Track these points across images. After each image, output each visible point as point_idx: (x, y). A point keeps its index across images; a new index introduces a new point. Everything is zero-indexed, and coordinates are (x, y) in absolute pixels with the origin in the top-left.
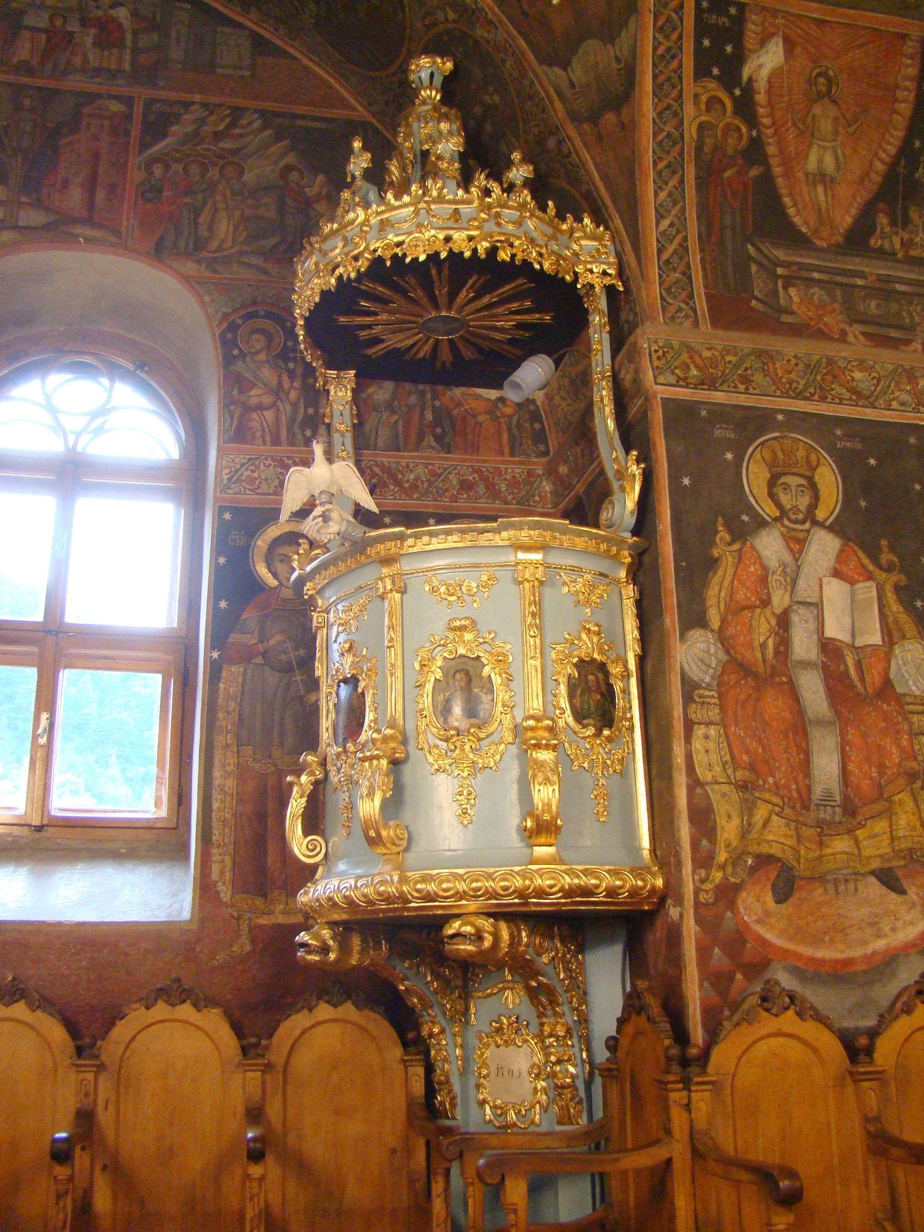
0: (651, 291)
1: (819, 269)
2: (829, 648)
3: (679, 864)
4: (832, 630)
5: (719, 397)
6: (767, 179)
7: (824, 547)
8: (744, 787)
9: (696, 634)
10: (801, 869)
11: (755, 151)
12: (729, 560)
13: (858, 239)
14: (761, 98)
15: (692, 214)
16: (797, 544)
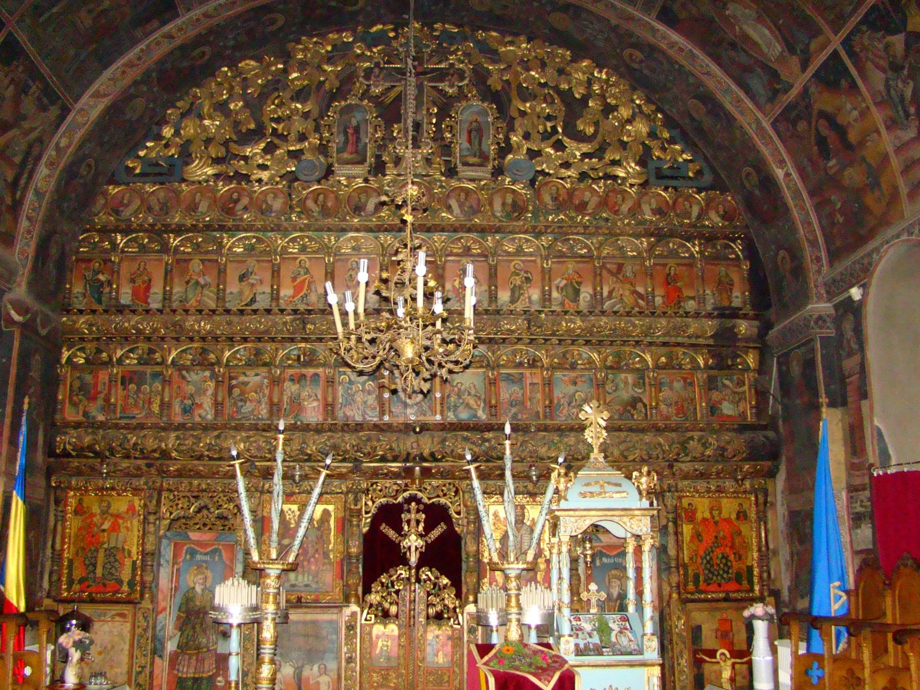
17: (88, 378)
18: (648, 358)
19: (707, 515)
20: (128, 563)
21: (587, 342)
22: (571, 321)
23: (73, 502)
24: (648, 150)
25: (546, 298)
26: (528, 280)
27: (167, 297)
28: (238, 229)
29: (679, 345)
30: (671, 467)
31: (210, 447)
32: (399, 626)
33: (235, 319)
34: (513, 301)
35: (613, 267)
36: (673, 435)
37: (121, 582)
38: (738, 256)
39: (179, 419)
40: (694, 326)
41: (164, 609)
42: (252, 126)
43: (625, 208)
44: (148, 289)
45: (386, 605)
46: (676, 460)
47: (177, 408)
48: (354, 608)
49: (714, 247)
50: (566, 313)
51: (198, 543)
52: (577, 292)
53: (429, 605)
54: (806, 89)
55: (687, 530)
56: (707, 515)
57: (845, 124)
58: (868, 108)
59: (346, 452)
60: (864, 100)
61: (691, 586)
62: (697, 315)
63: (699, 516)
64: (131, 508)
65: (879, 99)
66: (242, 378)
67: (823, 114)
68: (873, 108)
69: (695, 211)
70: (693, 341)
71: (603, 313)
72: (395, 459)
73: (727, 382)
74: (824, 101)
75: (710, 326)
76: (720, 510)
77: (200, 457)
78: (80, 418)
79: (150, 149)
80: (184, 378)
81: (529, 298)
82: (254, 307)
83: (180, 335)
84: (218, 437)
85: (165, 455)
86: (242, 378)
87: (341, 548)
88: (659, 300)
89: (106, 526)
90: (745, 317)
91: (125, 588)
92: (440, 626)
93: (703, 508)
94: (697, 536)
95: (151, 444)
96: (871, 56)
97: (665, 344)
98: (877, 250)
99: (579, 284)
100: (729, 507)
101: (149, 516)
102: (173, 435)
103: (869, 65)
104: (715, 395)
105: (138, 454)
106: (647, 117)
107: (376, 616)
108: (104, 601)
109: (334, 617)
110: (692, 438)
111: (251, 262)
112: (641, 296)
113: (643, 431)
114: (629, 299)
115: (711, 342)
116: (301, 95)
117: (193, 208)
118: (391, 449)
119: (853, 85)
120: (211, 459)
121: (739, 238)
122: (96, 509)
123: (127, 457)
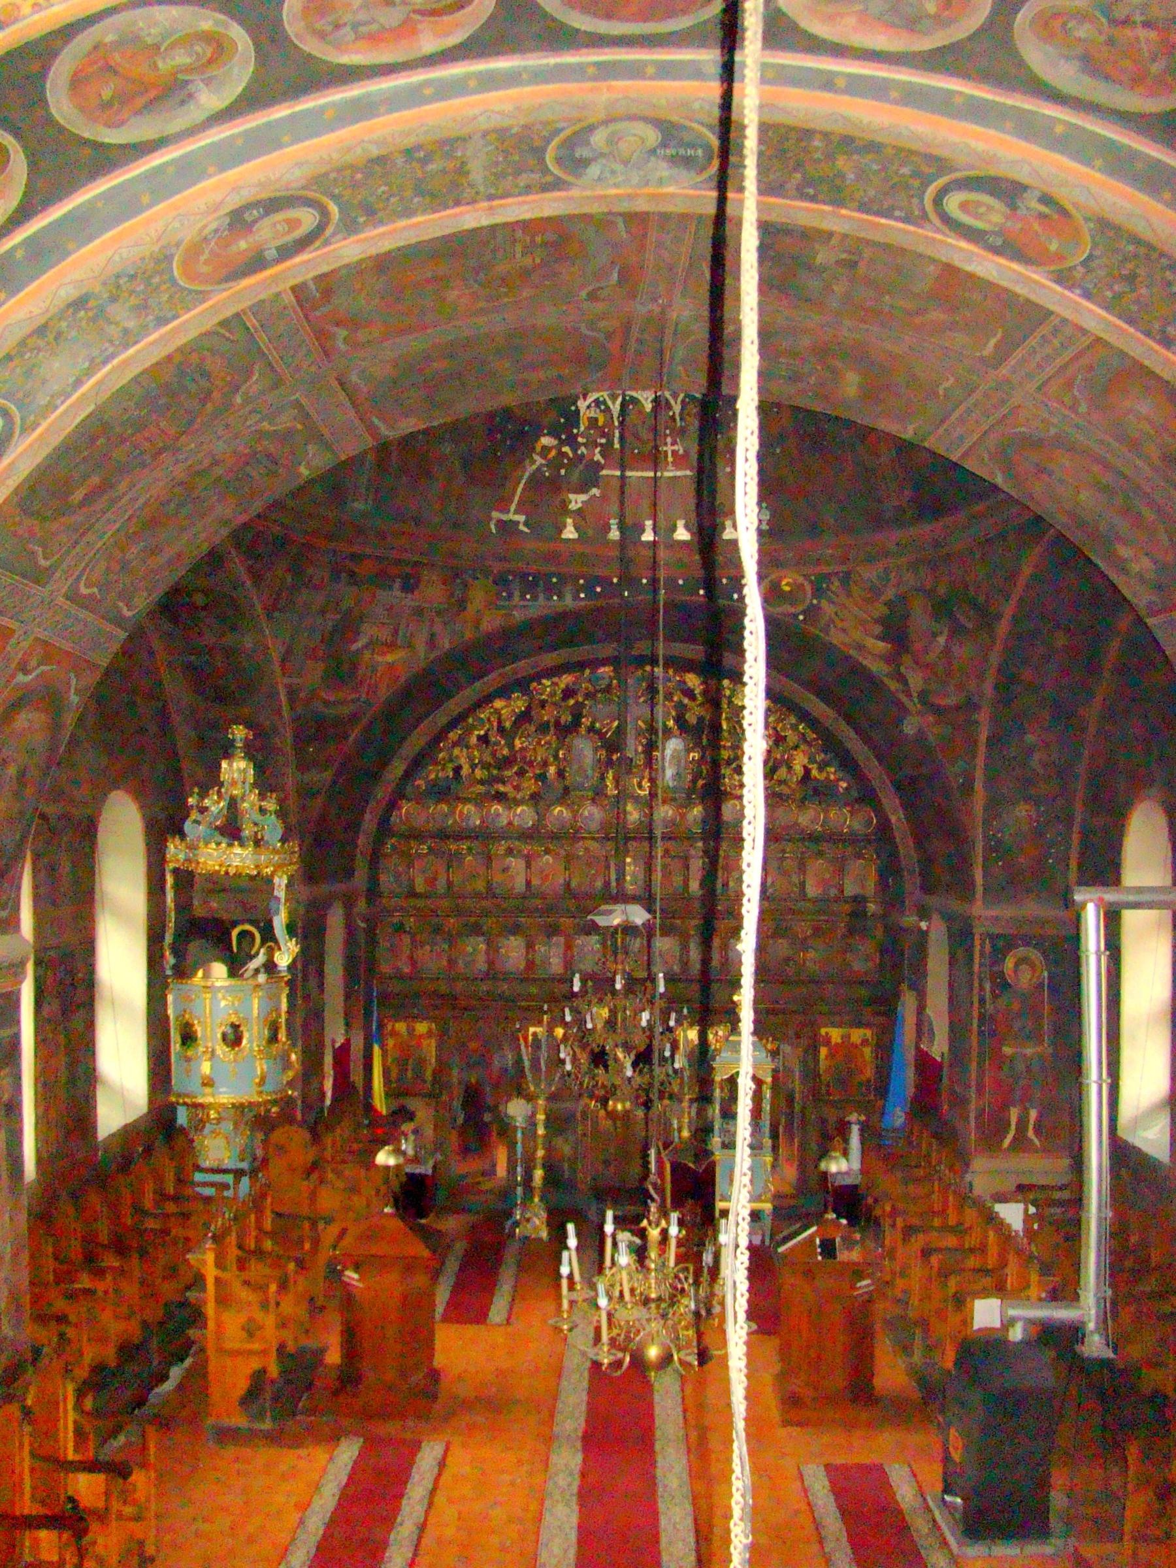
23: (389, 1027)
24: (807, 771)
27: (450, 884)
42: (506, 752)
44: (435, 879)
47: (461, 963)
48: (587, 1100)
55: (824, 1051)
63: (833, 1041)
64: (430, 1031)
76: (849, 1036)
79: (432, 773)
93: (836, 1034)
94: (831, 1055)
101: (442, 1035)
106: (809, 744)
116: (543, 728)
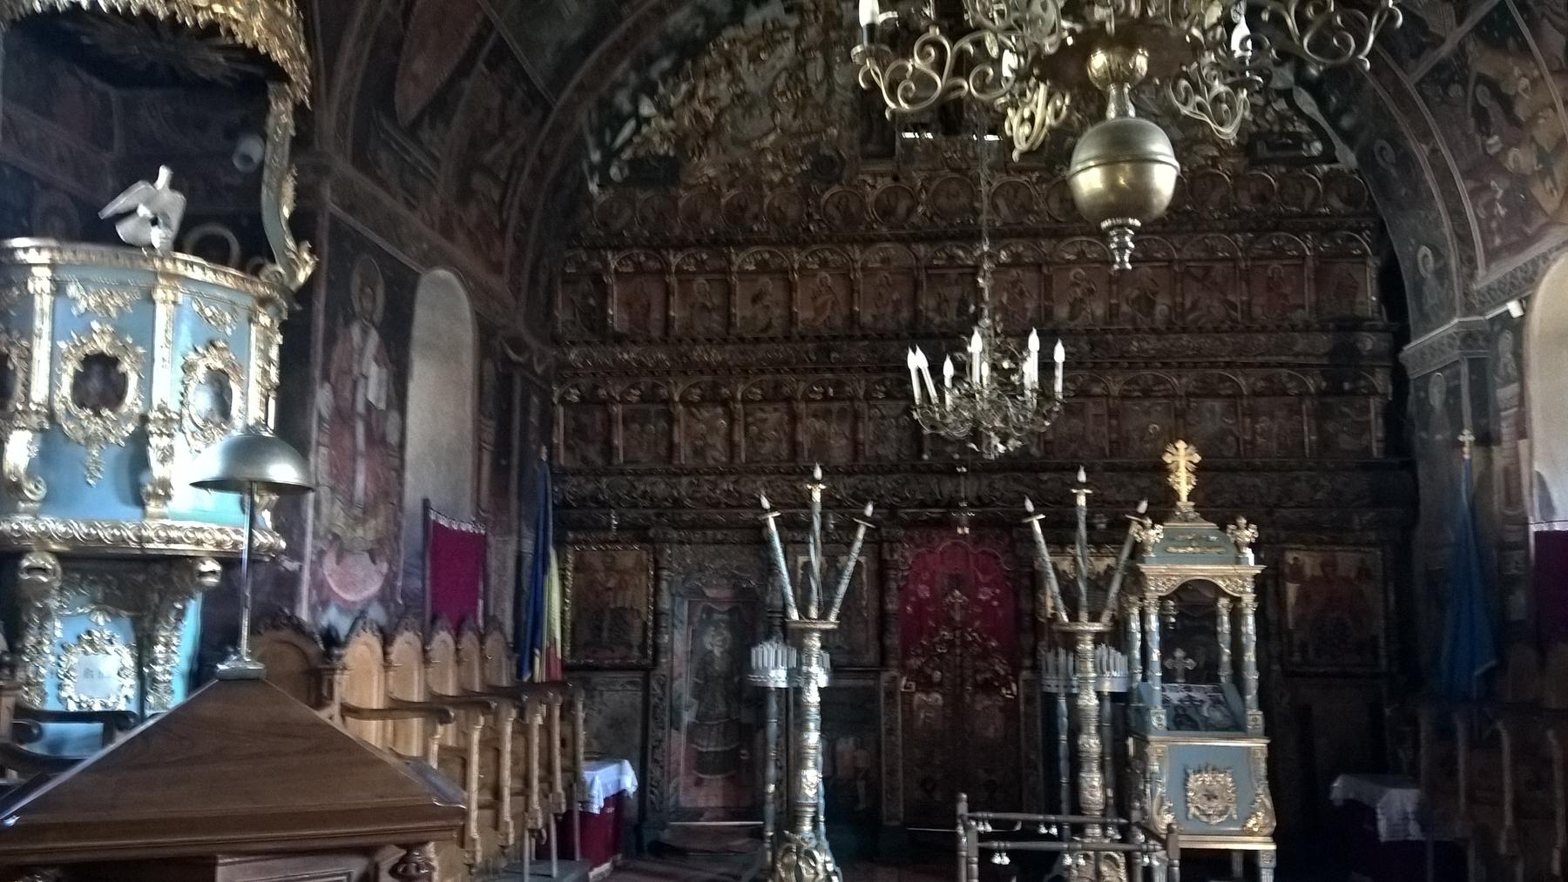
0: (328, 122)
1: (397, 143)
2: (368, 405)
3: (303, 534)
4: (371, 398)
5: (351, 220)
6: (395, 67)
7: (374, 338)
8: (333, 489)
9: (327, 386)
10: (346, 546)
11: (398, 46)
12: (341, 337)
13: (413, 129)
14: (415, 10)
15: (360, 75)
16: (365, 332)
17: (585, 419)
18: (1242, 381)
19: (1318, 572)
20: (637, 623)
21: (1165, 365)
22: (1144, 339)
25: (1113, 312)
26: (1091, 291)
28: (749, 243)
29: (1281, 365)
30: (1269, 514)
31: (728, 493)
32: (943, 695)
33: (749, 347)
34: (1072, 317)
35: (1199, 273)
36: (1275, 475)
37: (630, 646)
38: (1365, 251)
39: (691, 463)
40: (1301, 343)
41: (680, 675)
43: (1215, 197)
45: (929, 671)
46: (1277, 506)
49: (1333, 240)
50: (1137, 330)
51: (714, 600)
52: (1152, 304)
53: (977, 671)
54: (1461, 46)
55: (1292, 590)
56: (1318, 572)
57: (1512, 93)
58: (1542, 77)
59: (881, 496)
60: (1537, 65)
61: (1297, 658)
62: (1307, 328)
63: (1308, 572)
64: (639, 560)
65: (1556, 67)
66: (760, 415)
67: (1482, 79)
68: (1549, 79)
69: (1309, 194)
70: (1301, 360)
71: (1184, 330)
72: (936, 506)
73: (1346, 410)
74: (1484, 63)
75: (1323, 342)
76: (1334, 565)
77: (717, 505)
78: (579, 464)
80: (693, 415)
81: (1093, 314)
82: (771, 333)
83: (687, 368)
84: (735, 482)
85: (678, 503)
86: (760, 415)
87: (876, 604)
88: (1257, 311)
89: (611, 583)
90: (1372, 329)
91: (636, 653)
92: (989, 695)
94: (1303, 597)
95: (661, 489)
96: (1548, 12)
97: (1262, 365)
98: (1545, 258)
99: (1154, 294)
100: (1347, 560)
102: (685, 480)
103: (1546, 24)
104: (1330, 427)
105: (647, 503)
107: (918, 684)
108: (614, 668)
109: (871, 683)
110: (1297, 479)
111: (765, 279)
112: (1233, 306)
113: (1234, 470)
114: (1218, 310)
115: (1325, 361)
117: (693, 217)
118: (932, 493)
119: (1524, 48)
120: (728, 506)
121: (1368, 228)
122: (598, 564)
123: (635, 506)
